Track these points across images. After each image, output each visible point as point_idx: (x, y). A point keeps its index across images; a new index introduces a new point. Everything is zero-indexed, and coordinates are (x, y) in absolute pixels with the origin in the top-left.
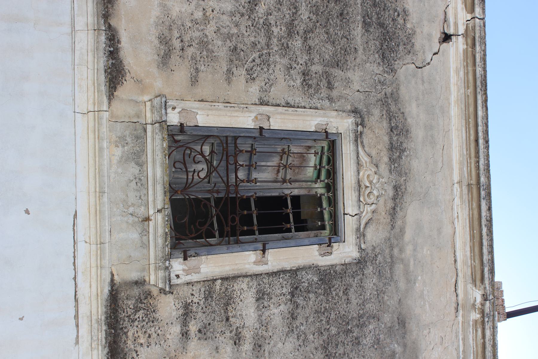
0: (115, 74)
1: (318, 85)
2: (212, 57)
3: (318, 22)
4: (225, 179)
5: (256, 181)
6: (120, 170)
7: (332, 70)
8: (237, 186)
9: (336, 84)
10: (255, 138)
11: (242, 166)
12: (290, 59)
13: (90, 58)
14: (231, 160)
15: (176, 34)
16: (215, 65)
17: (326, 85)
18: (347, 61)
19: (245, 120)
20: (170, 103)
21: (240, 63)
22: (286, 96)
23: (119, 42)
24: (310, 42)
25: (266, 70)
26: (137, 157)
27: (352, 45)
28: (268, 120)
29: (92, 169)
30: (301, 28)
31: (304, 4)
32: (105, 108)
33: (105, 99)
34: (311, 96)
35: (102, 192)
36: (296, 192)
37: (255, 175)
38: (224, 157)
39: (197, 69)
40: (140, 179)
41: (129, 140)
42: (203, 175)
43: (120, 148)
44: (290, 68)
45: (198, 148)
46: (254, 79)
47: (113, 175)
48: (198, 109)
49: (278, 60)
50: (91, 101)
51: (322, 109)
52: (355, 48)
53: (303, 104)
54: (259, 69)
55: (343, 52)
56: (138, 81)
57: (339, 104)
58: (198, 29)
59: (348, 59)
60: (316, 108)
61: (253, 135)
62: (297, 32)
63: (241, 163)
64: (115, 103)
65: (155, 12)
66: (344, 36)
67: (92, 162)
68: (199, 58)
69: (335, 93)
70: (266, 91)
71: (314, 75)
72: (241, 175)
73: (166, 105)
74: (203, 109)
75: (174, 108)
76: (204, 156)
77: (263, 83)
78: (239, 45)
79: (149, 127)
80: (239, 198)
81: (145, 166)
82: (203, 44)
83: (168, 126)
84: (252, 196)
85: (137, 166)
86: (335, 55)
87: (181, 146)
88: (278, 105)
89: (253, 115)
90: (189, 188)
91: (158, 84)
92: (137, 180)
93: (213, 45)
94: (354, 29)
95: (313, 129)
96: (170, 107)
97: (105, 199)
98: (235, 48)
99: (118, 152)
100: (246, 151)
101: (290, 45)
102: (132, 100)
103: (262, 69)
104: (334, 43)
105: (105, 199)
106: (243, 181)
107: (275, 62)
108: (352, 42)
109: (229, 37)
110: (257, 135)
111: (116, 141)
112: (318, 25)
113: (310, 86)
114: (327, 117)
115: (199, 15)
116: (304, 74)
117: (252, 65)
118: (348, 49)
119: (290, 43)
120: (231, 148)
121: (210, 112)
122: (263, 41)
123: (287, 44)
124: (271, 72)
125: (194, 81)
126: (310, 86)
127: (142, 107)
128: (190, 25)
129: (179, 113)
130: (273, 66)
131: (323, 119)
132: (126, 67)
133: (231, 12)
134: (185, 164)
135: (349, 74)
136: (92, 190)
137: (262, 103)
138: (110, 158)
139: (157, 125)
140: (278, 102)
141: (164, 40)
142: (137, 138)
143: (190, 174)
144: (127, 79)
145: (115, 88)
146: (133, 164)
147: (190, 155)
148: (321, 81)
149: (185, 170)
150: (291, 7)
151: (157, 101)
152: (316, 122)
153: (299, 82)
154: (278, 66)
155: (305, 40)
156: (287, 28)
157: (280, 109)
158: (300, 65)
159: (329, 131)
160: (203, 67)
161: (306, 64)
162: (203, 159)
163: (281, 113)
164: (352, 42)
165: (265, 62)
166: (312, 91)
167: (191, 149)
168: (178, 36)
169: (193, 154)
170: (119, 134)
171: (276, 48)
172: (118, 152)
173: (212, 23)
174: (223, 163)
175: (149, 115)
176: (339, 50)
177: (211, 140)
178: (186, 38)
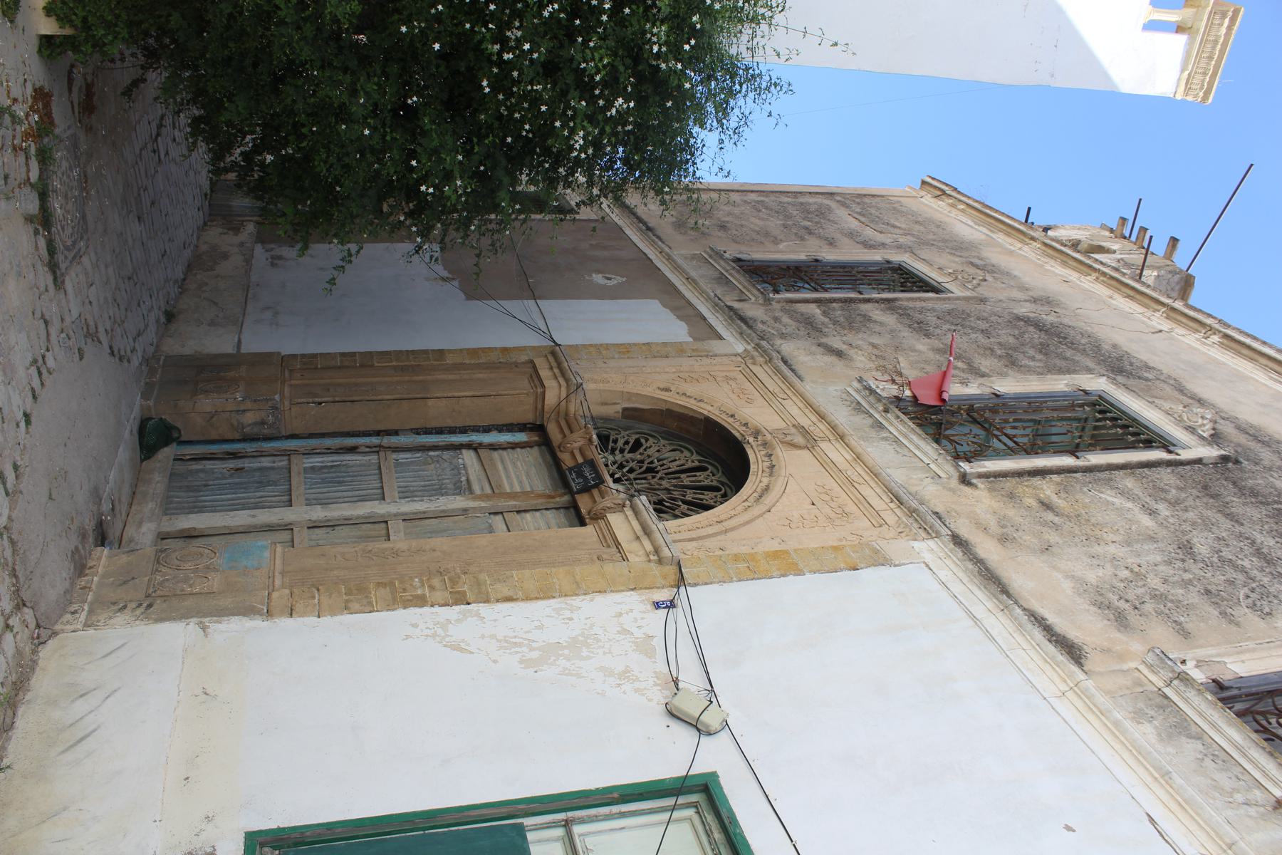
6: (1170, 749)
13: (1019, 639)
26: (1181, 727)
29: (1126, 755)
32: (1081, 676)
33: (1075, 669)
35: (1166, 775)
41: (1152, 713)
48: (1218, 655)
50: (1058, 681)
56: (1106, 651)
65: (1067, 585)
67: (1118, 747)
79: (1168, 691)
81: (1206, 737)
82: (1157, 597)
91: (1137, 646)
97: (1179, 781)
105: (1179, 781)
115: (1125, 574)
127: (1137, 674)
136: (1149, 780)
141: (1103, 606)
142: (1162, 707)
146: (1184, 739)
151: (1150, 658)
170: (1131, 709)
173: (1150, 576)
175: (1153, 678)
178: (1131, 596)
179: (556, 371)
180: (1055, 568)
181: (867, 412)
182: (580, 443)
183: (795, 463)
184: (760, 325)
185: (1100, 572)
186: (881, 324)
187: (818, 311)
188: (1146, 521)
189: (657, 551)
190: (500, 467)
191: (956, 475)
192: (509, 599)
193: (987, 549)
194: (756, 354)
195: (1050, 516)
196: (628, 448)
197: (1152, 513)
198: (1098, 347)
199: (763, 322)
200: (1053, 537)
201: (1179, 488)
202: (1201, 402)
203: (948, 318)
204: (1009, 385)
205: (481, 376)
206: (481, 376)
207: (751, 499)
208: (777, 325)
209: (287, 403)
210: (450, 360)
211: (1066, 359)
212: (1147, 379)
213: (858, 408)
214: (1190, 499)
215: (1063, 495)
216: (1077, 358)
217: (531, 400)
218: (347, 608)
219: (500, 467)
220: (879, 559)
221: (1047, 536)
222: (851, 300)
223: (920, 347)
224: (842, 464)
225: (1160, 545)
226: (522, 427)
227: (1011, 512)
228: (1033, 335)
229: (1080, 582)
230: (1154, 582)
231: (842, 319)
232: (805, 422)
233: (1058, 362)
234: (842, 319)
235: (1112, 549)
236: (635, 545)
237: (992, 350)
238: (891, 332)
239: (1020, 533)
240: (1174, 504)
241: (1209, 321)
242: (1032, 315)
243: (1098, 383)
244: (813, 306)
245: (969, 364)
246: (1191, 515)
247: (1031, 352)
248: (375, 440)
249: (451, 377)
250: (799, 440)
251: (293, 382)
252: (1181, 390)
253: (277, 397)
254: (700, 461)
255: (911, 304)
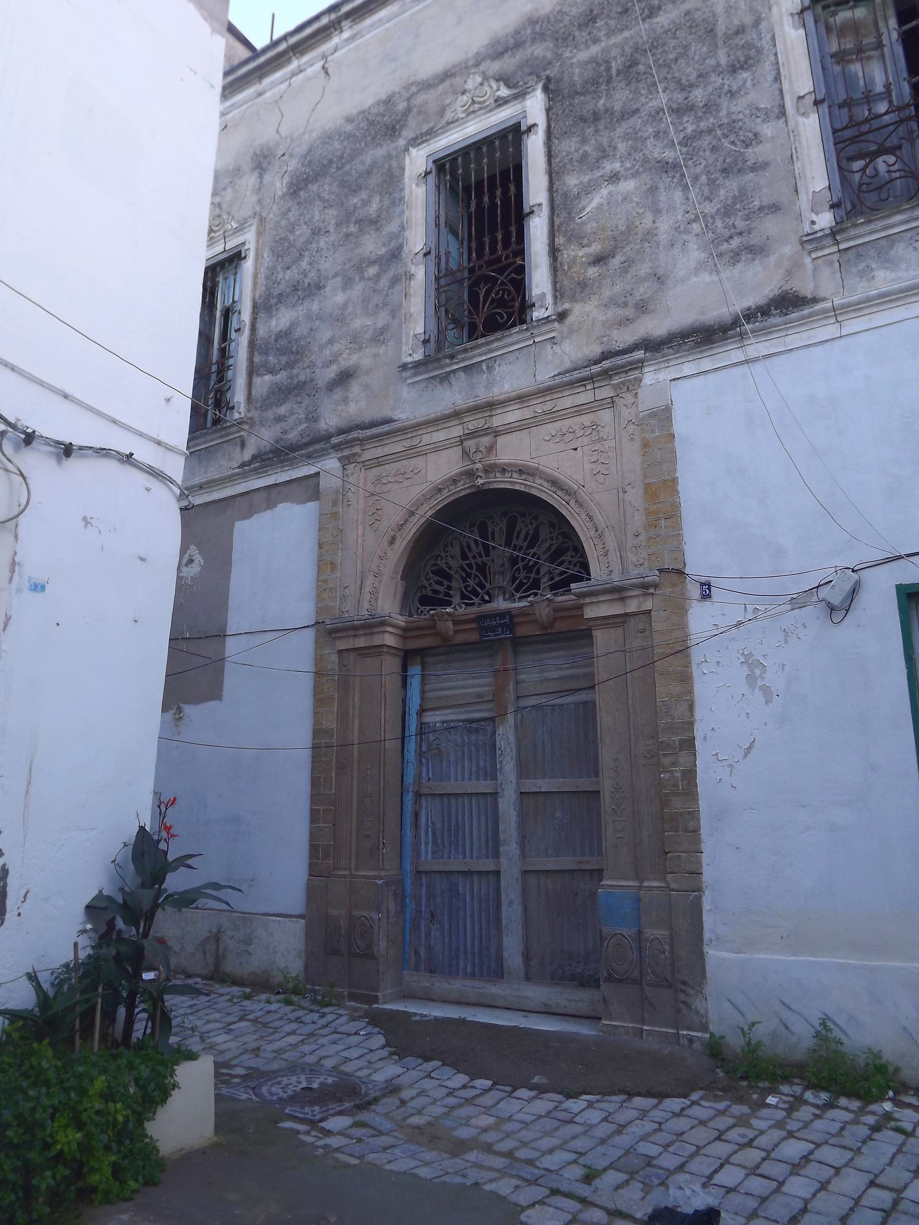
0: (787, 303)
1: (743, 47)
2: (742, 195)
3: (666, 78)
4: (892, 128)
5: (888, 86)
6: (903, 266)
7: (720, 35)
8: (899, 109)
9: (737, 22)
10: (830, 106)
11: (870, 110)
12: (720, 97)
14: (865, 128)
15: (725, 246)
16: (750, 189)
17: (740, 36)
18: (703, 21)
19: (810, 129)
20: (807, 229)
21: (740, 159)
22: (767, 85)
23: (749, 309)
24: (693, 78)
25: (740, 124)
27: (682, 21)
28: (803, 97)
30: (679, 96)
31: (650, 105)
34: (759, 51)
36: (893, 22)
37: (879, 88)
38: (863, 138)
39: (759, 209)
40: (911, 238)
41: (862, 266)
42: (891, 159)
43: (875, 273)
44: (732, 94)
45: (857, 176)
46: (756, 135)
47: (912, 273)
48: (807, 193)
49: (724, 112)
51: (772, 30)
52: (685, 15)
53: (772, 58)
54: (741, 133)
55: (694, 30)
56: (789, 273)
57: (759, 8)
58: (713, 223)
59: (700, 19)
60: (773, 38)
61: (827, 110)
62: (686, 99)
63: (867, 113)
64: (821, 293)
66: (675, 37)
68: (746, 211)
69: (748, 20)
70: (766, 113)
71: (732, 57)
72: (882, 107)
73: (811, 234)
74: (807, 187)
75: (813, 222)
76: (866, 166)
77: (759, 120)
78: (719, 167)
79: (843, 246)
80: (915, 100)
82: (727, 211)
83: (837, 223)
84: (908, 82)
85: (895, 247)
86: (701, 40)
87: (859, 199)
88: (781, 91)
89: (801, 120)
90: (912, 172)
92: (912, 241)
93: (727, 199)
94: (662, 27)
95: (802, 32)
96: (812, 228)
98: (724, 171)
99: (880, 274)
100: (850, 111)
101: (703, 103)
102: (814, 276)
103: (741, 128)
104: (686, 46)
106: (891, 102)
107: (729, 114)
108: (678, 22)
109: (712, 182)
110: (825, 105)
111: (868, 280)
112: (669, 76)
113: (748, 58)
114: (781, 17)
116: (734, 72)
117: (738, 143)
118: (688, 24)
119: (701, 105)
120: (847, 134)
121: (809, 176)
122: (706, 141)
123: (703, 107)
124: (741, 116)
125: (774, 208)
126: (748, 58)
128: (710, 234)
129: (817, 214)
130: (734, 116)
131: (786, 23)
132: (776, 293)
133: (683, 190)
134: (880, 188)
135: (720, 9)
137: (782, 113)
138: (891, 282)
139: (838, 238)
140: (777, 92)
141: (735, 257)
143: (894, 175)
144: (789, 288)
145: (804, 298)
147: (868, 184)
148: (737, 45)
149: (889, 185)
150: (658, 118)
152: (792, 31)
153: (745, 75)
154: (733, 109)
155: (692, 86)
156: (684, 114)
157: (786, 87)
158: (725, 81)
159: (800, 8)
160: (756, 203)
161: (720, 73)
162: (871, 165)
163: (791, 83)
164: (678, 22)
165: (732, 126)
166: (753, 53)
167: (861, 185)
168: (726, 244)
169: (866, 180)
170: (858, 279)
171: (712, 120)
172: (880, 274)
174: (870, 137)
176: (692, 36)
177: (844, 163)
178: (727, 233)
179: (361, 632)
180: (684, 280)
181: (449, 373)
182: (450, 624)
183: (512, 450)
184: (290, 436)
185: (693, 246)
186: (294, 325)
187: (267, 378)
188: (628, 186)
189: (645, 586)
190: (448, 693)
191: (556, 324)
192: (691, 707)
193: (656, 326)
194: (346, 452)
195: (616, 262)
196: (446, 583)
197: (614, 178)
198: (349, 136)
199: (285, 432)
200: (644, 269)
201: (584, 141)
202: (446, 75)
203: (288, 260)
204: (417, 238)
205: (357, 698)
206: (357, 698)
207: (567, 498)
208: (291, 421)
209: (383, 873)
210: (331, 723)
211: (369, 172)
212: (409, 110)
213: (445, 379)
214: (600, 139)
215: (585, 241)
216: (368, 161)
217: (388, 657)
218: (696, 831)
219: (448, 693)
220: (664, 415)
221: (642, 273)
222: (252, 345)
223: (340, 298)
224: (527, 413)
225: (661, 185)
226: (405, 668)
227: (607, 293)
228: (326, 188)
229: (700, 267)
230: (710, 208)
231: (284, 359)
232: (457, 431)
233: (375, 179)
234: (284, 359)
235: (664, 226)
236: (628, 601)
237: (348, 235)
238: (309, 317)
239: (636, 294)
240: (604, 154)
241: (325, 21)
242: (286, 179)
243: (418, 160)
244: (257, 380)
245: (372, 263)
246: (622, 147)
247: (355, 200)
248: (409, 798)
249: (356, 725)
250: (486, 440)
251: (353, 867)
252: (427, 85)
253: (380, 882)
254: (472, 525)
255: (261, 289)
